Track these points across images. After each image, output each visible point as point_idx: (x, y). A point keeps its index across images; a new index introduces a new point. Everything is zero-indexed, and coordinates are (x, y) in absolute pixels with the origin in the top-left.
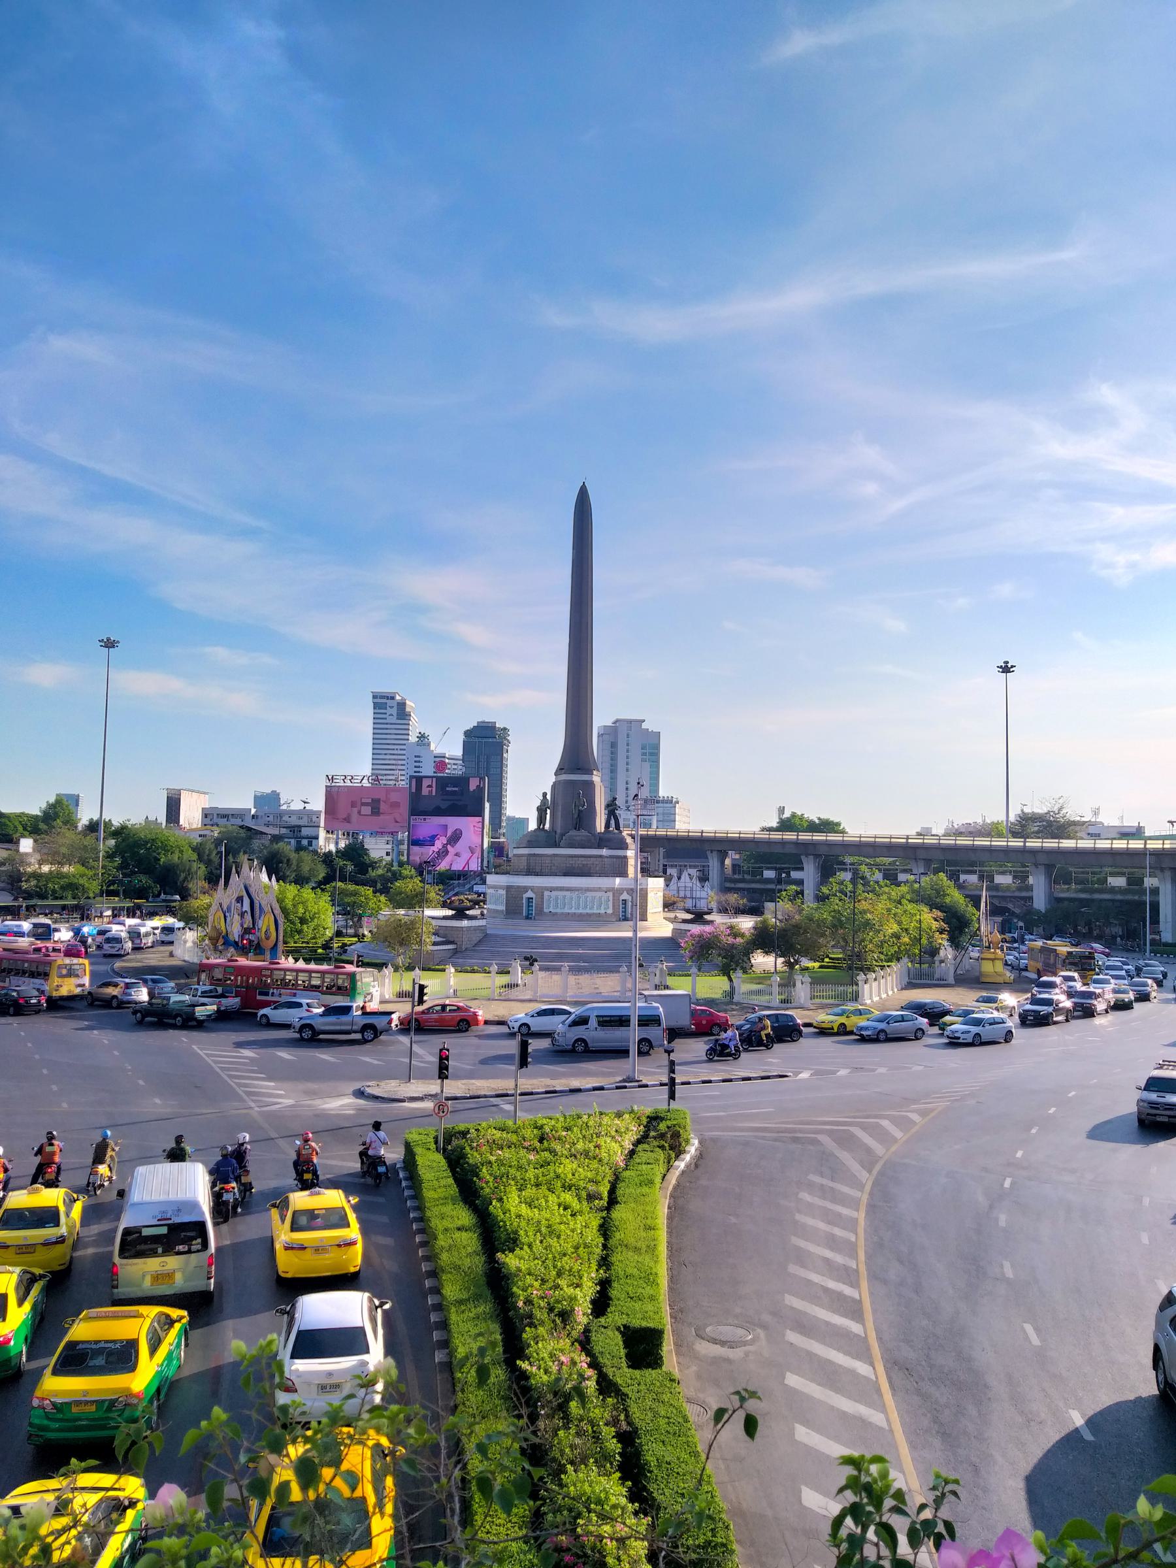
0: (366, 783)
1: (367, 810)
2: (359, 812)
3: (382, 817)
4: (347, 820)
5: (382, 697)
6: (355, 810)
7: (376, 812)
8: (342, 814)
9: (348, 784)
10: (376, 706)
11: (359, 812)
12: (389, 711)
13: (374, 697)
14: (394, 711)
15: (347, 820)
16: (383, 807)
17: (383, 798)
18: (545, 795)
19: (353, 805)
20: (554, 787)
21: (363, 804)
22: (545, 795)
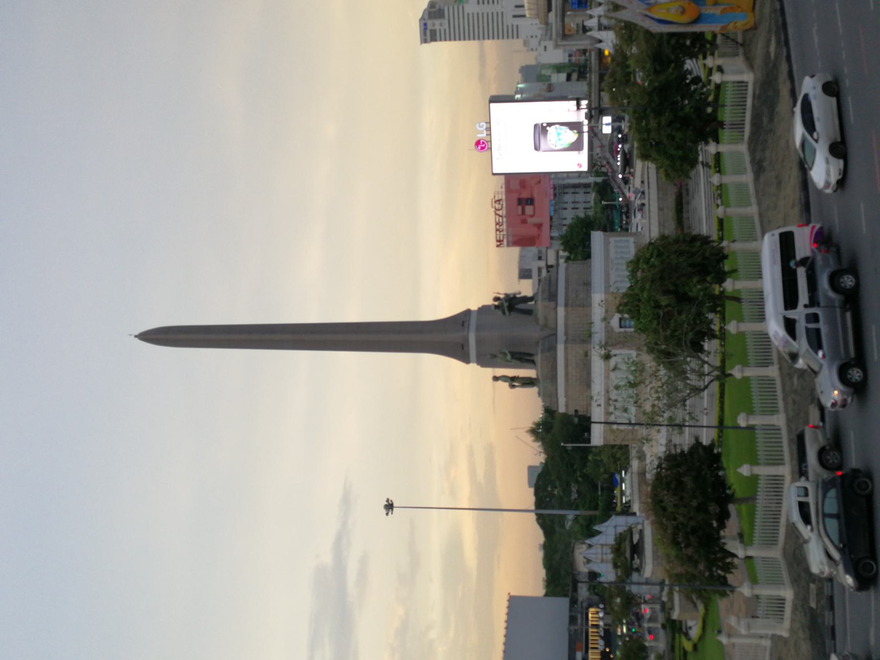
0: (503, 212)
1: (529, 209)
2: (532, 216)
3: (536, 196)
4: (539, 226)
5: (425, 34)
6: (529, 220)
7: (530, 201)
8: (534, 231)
9: (504, 227)
10: (433, 38)
11: (532, 216)
12: (437, 27)
13: (424, 41)
14: (437, 22)
15: (539, 226)
16: (525, 195)
17: (515, 196)
18: (496, 379)
19: (524, 222)
20: (483, 361)
21: (523, 212)
22: (496, 379)
